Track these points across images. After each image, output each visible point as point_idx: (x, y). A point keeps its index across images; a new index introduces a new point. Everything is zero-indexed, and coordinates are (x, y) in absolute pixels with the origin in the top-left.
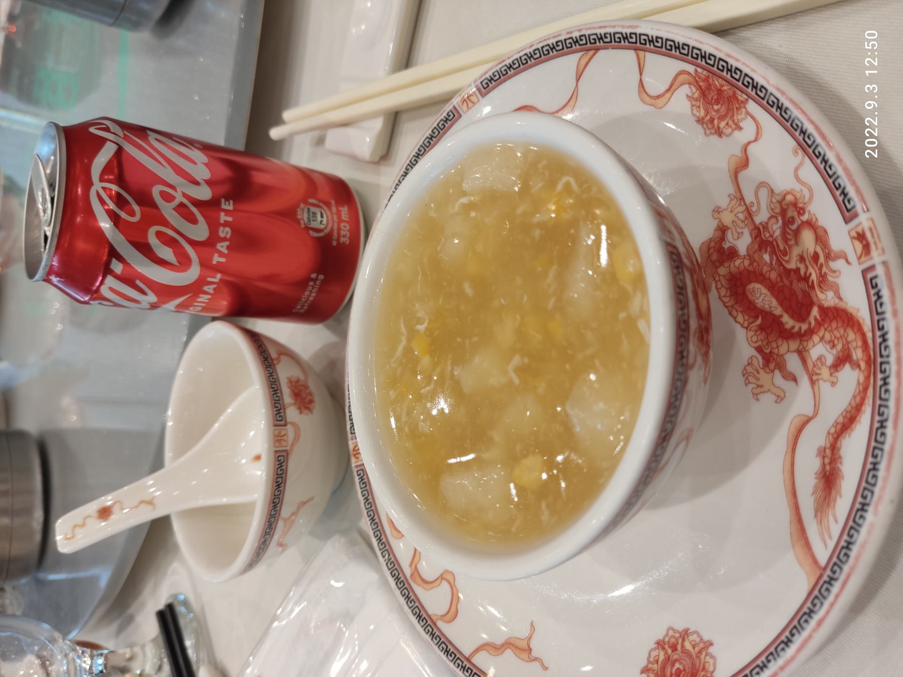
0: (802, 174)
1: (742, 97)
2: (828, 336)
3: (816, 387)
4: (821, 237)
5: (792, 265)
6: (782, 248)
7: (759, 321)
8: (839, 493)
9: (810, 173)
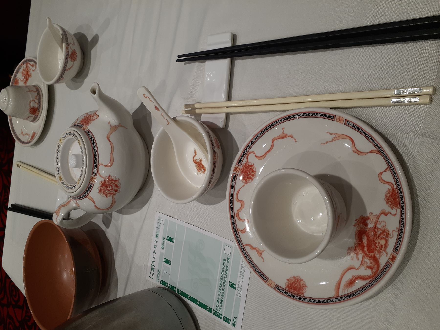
2: (371, 261)
4: (386, 245)
5: (376, 242)
6: (377, 236)
8: (351, 287)
9: (396, 235)
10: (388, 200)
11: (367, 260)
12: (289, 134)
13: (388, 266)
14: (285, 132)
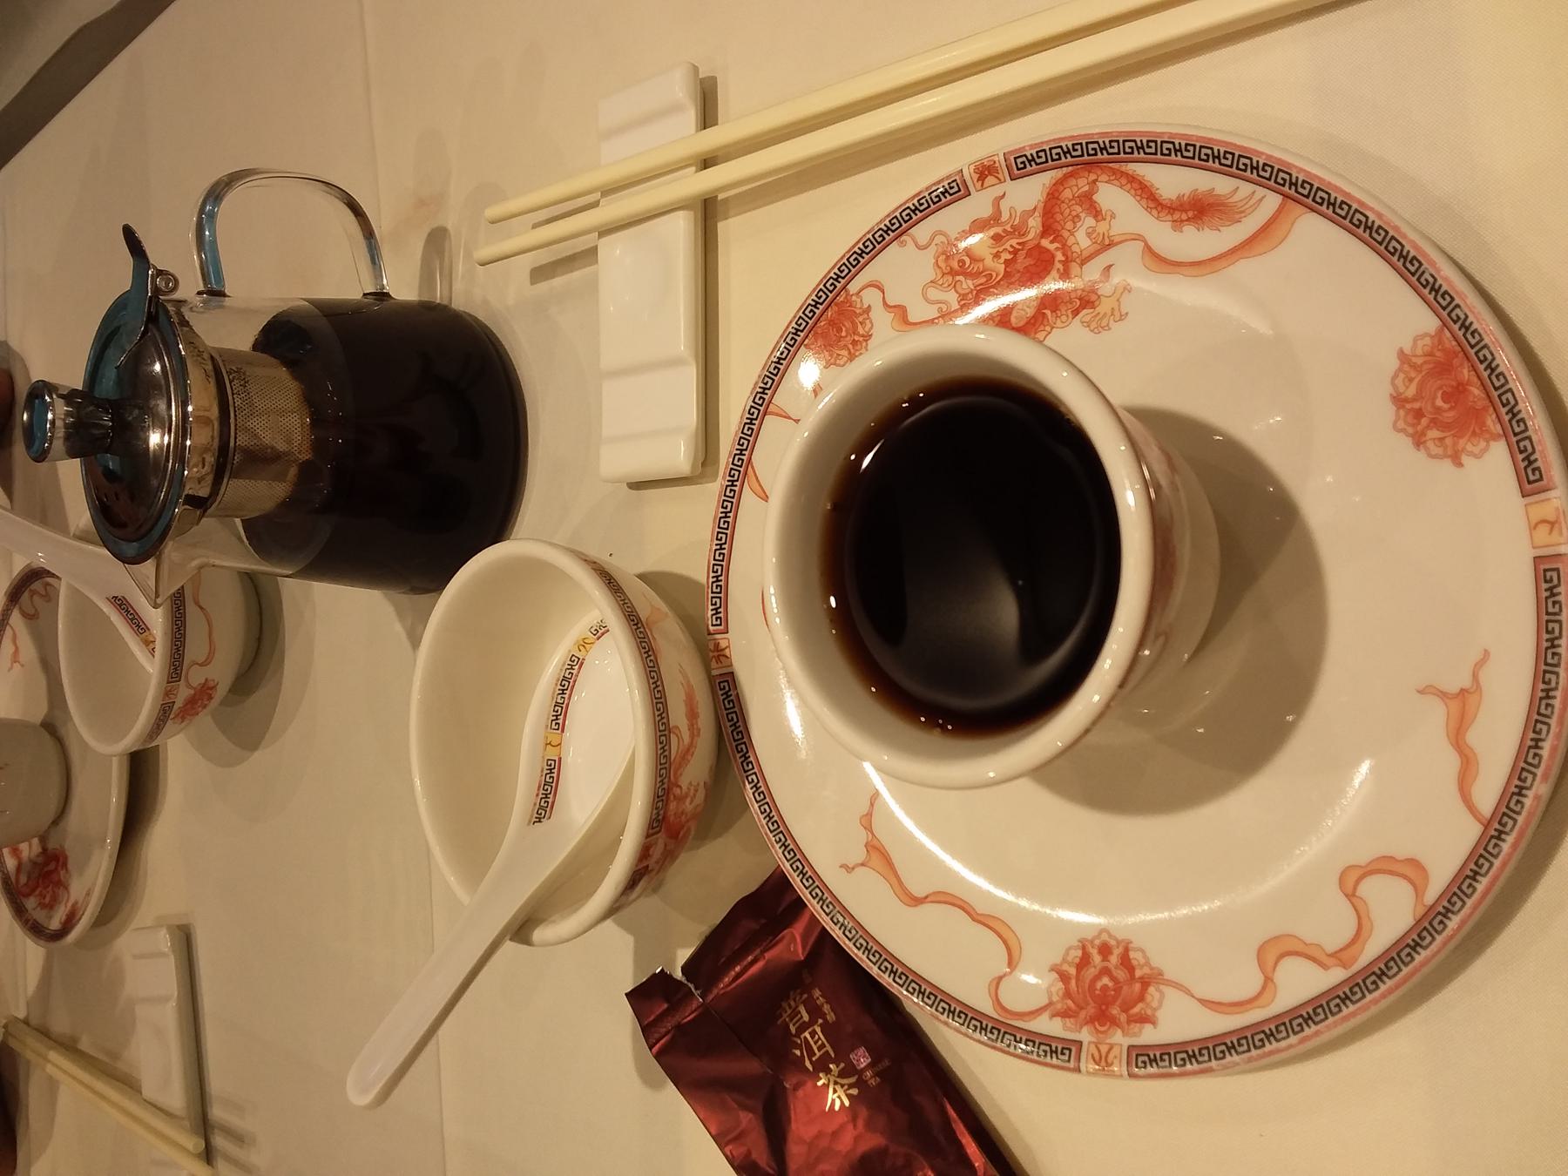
0: (923, 241)
1: (840, 299)
2: (1069, 225)
3: (1117, 239)
6: (983, 280)
7: (1048, 312)
9: (922, 231)
10: (854, 343)
11: (1081, 240)
12: (863, 836)
13: (1024, 164)
14: (859, 854)
